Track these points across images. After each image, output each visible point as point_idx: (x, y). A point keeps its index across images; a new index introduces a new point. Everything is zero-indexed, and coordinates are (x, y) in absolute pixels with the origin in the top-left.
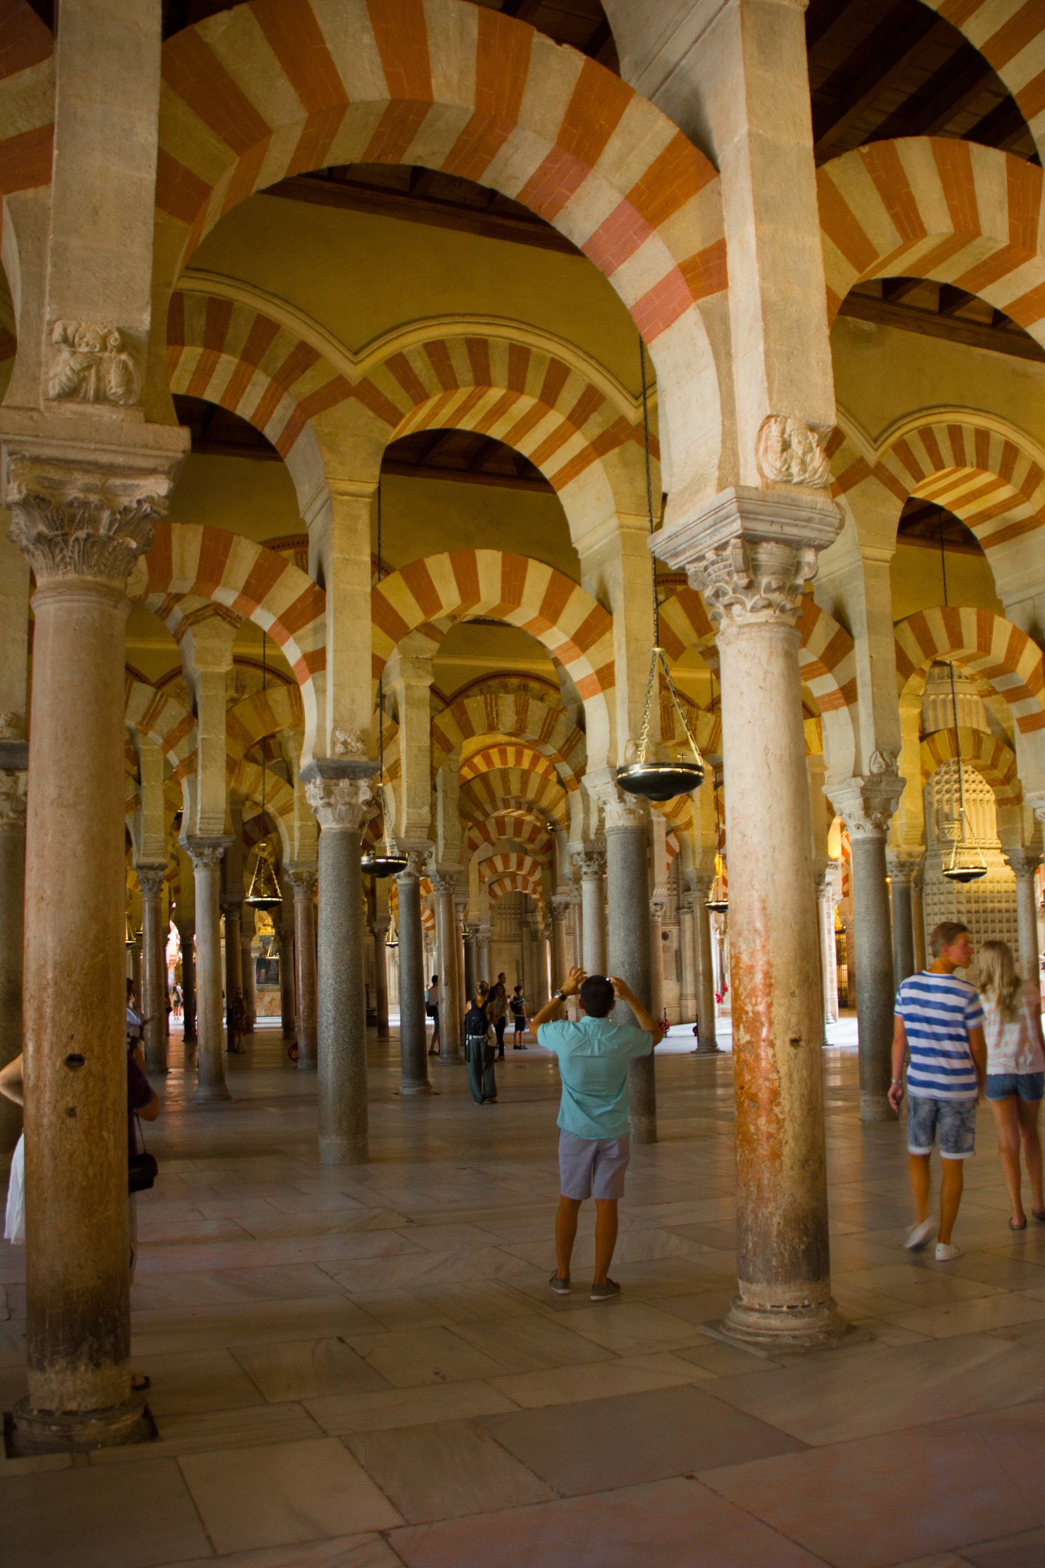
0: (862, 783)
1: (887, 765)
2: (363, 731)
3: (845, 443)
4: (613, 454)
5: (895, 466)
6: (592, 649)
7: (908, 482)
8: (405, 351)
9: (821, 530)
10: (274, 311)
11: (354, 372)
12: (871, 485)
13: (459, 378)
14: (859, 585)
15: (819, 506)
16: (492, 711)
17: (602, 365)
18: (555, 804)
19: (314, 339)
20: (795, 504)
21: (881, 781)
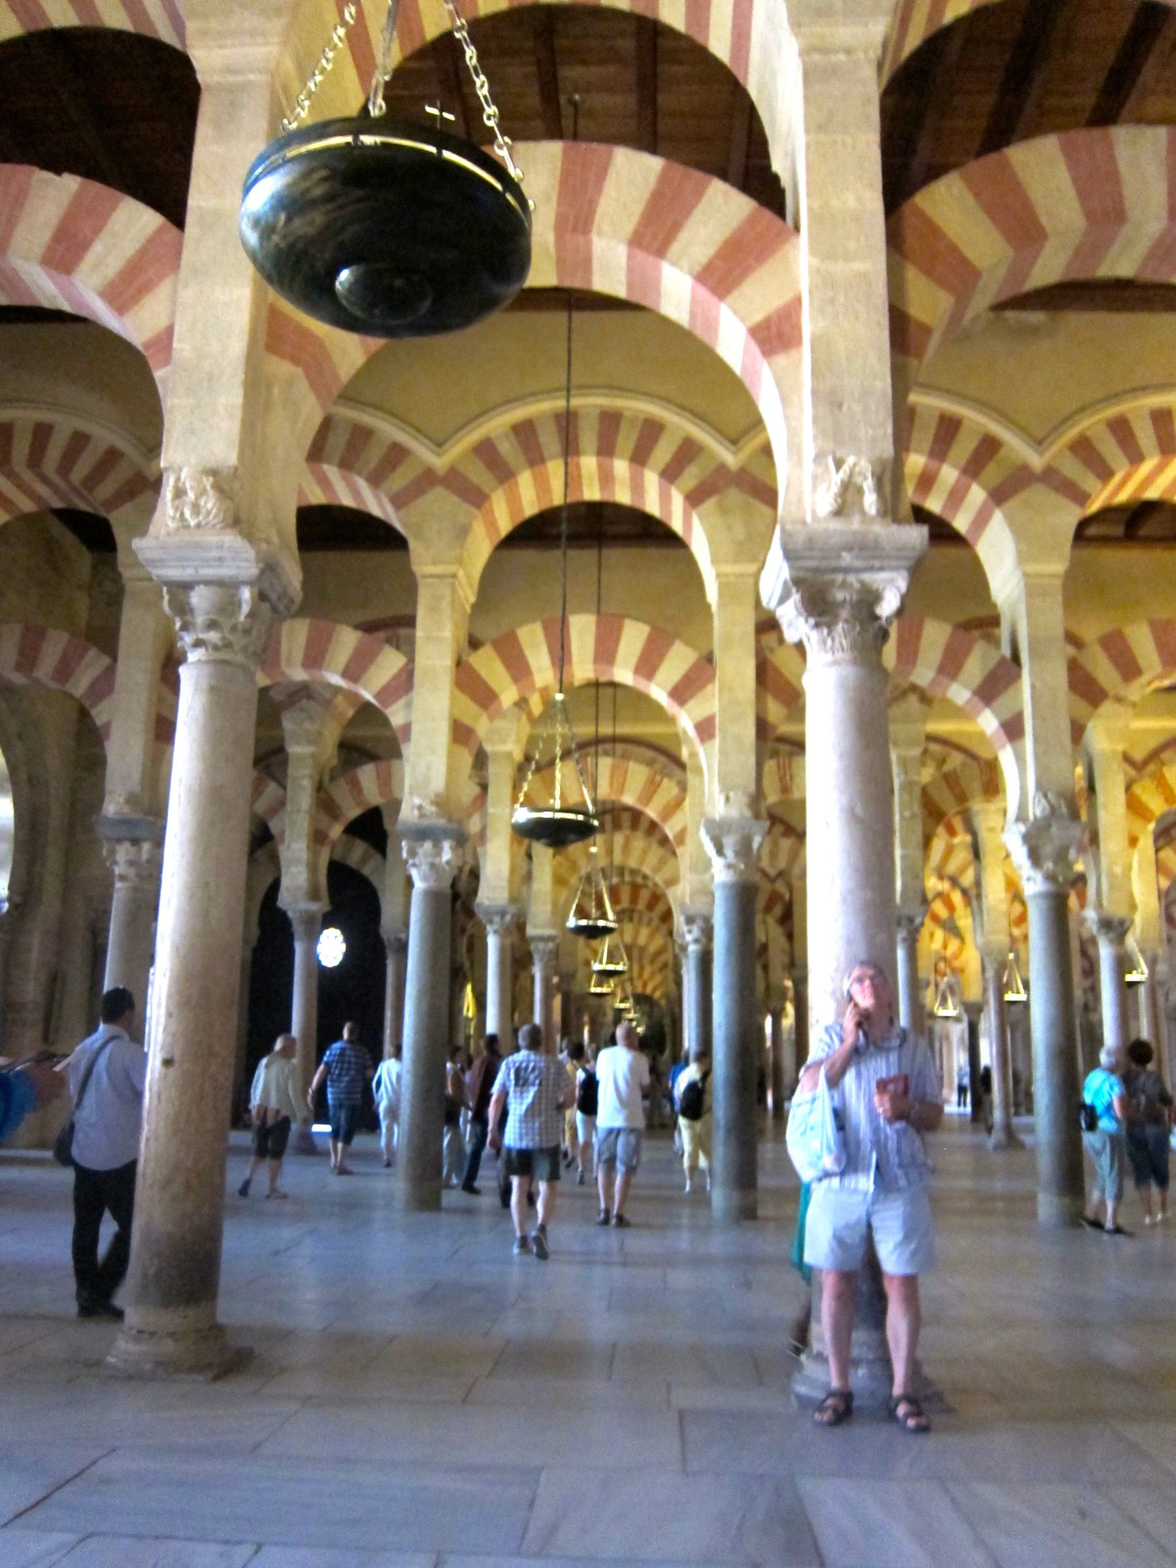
0: (1022, 828)
1: (1053, 809)
2: (438, 795)
3: (1003, 453)
4: (710, 504)
5: (1072, 469)
6: (692, 704)
7: (1088, 481)
8: (493, 435)
9: (237, 567)
10: (367, 418)
11: (440, 462)
12: (1038, 494)
13: (546, 453)
14: (1022, 609)
15: (226, 545)
16: (785, 772)
17: (698, 416)
18: (963, 870)
19: (403, 437)
20: (198, 546)
21: (1050, 826)
